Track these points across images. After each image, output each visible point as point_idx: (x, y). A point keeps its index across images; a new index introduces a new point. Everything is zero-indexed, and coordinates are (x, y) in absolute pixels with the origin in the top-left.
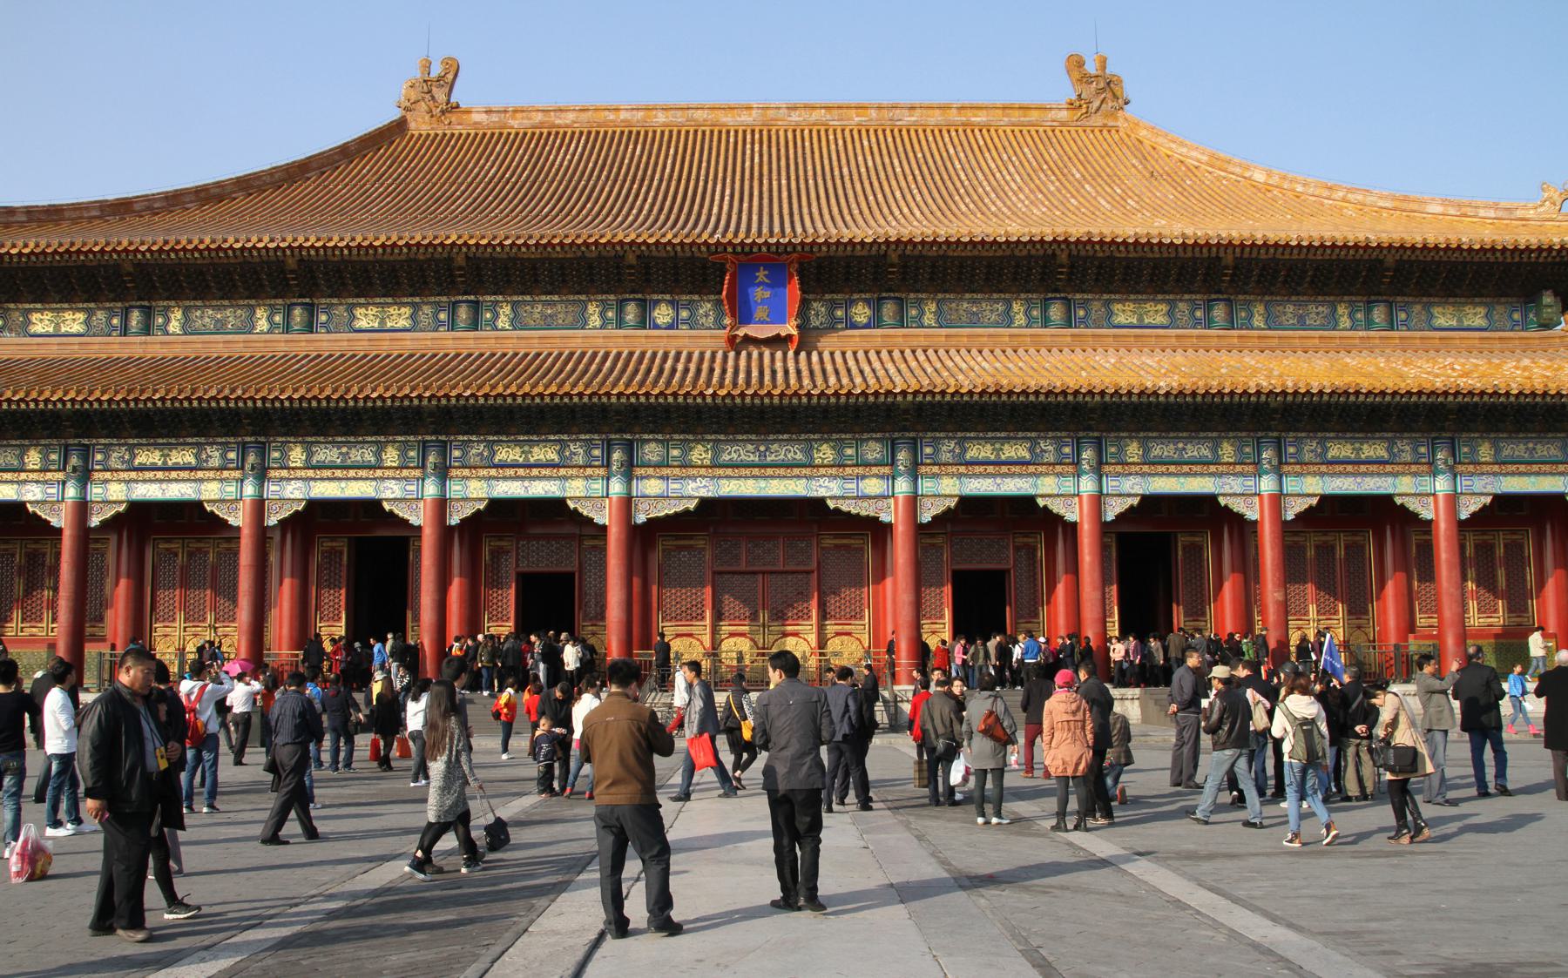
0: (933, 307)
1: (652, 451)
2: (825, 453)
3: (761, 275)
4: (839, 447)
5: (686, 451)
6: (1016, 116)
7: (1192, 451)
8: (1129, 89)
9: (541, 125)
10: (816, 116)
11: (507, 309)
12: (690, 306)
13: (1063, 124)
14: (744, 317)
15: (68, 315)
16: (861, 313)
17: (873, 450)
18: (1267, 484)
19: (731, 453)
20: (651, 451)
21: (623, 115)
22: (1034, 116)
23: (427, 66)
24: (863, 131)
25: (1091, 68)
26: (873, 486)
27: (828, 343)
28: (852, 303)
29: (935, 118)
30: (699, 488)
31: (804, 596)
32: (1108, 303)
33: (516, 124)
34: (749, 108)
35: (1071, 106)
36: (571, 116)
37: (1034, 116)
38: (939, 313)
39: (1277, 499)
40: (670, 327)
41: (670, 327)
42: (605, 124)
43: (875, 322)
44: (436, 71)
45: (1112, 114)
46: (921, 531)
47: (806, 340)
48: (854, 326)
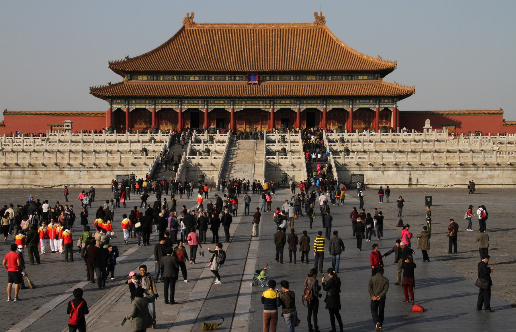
1: (237, 102)
2: (261, 102)
7: (313, 102)
8: (326, 20)
9: (211, 27)
10: (264, 26)
11: (213, 77)
12: (242, 77)
14: (250, 80)
16: (268, 78)
17: (268, 102)
18: (324, 107)
19: (248, 102)
20: (237, 102)
21: (227, 26)
22: (307, 26)
24: (274, 30)
25: (319, 15)
26: (268, 107)
27: (262, 84)
28: (266, 77)
29: (287, 26)
30: (244, 107)
31: (259, 122)
33: (206, 27)
34: (251, 24)
35: (315, 23)
36: (217, 26)
37: (307, 26)
38: (280, 78)
39: (326, 109)
41: (239, 80)
42: (223, 27)
43: (270, 80)
44: (190, 15)
45: (322, 25)
46: (274, 113)
47: (259, 84)
48: (267, 80)
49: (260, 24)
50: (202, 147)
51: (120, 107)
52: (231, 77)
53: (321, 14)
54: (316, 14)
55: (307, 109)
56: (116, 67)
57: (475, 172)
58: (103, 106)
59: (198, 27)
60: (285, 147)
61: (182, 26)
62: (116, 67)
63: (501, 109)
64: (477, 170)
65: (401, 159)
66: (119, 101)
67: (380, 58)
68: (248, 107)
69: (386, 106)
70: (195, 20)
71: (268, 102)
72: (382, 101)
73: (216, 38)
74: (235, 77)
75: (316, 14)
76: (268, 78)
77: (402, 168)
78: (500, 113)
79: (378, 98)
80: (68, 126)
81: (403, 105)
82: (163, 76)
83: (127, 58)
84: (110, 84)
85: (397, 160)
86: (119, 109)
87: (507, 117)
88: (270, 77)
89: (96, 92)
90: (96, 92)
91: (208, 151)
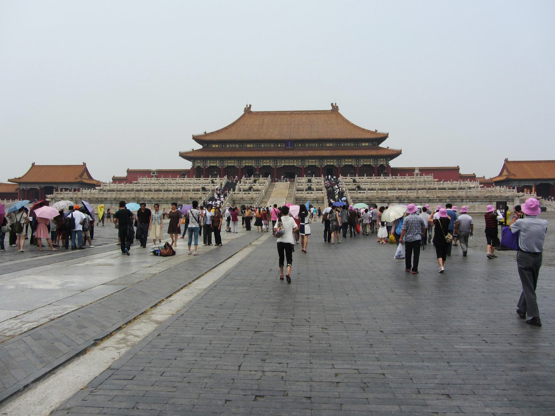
16: (300, 145)
23: (247, 105)
30: (283, 164)
49: (295, 111)
50: (247, 187)
53: (336, 104)
54: (332, 104)
55: (327, 166)
56: (197, 139)
57: (460, 203)
58: (187, 165)
61: (243, 112)
62: (197, 139)
63: (458, 166)
64: (462, 202)
65: (403, 194)
67: (376, 131)
70: (251, 110)
73: (266, 120)
74: (278, 145)
75: (332, 104)
76: (300, 145)
77: (404, 200)
78: (457, 169)
79: (376, 158)
80: (154, 173)
81: (394, 163)
83: (205, 133)
84: (193, 150)
85: (400, 194)
86: (199, 167)
87: (462, 172)
89: (184, 156)
90: (184, 156)
91: (250, 189)
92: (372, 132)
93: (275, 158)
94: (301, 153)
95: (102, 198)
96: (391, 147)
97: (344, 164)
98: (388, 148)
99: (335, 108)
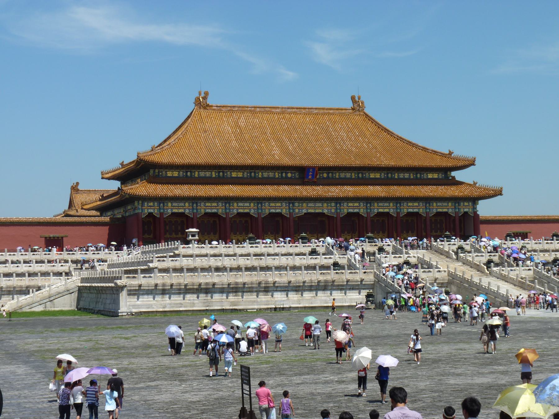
0: (338, 174)
1: (297, 204)
2: (325, 205)
3: (311, 170)
4: (327, 203)
5: (302, 205)
6: (340, 111)
8: (365, 104)
11: (260, 173)
12: (295, 173)
13: (350, 113)
15: (175, 172)
17: (333, 204)
20: (297, 204)
28: (323, 173)
30: (304, 211)
32: (369, 173)
35: (353, 109)
40: (291, 178)
44: (203, 95)
51: (152, 211)
52: (282, 173)
54: (353, 98)
59: (214, 110)
60: (492, 257)
66: (151, 204)
67: (450, 153)
68: (310, 211)
69: (466, 210)
70: (210, 101)
71: (333, 204)
72: (462, 203)
74: (286, 173)
76: (325, 175)
81: (485, 209)
82: (199, 172)
86: (150, 215)
88: (328, 174)
92: (443, 155)
93: (291, 200)
94: (335, 191)
95: (207, 284)
96: (482, 182)
97: (405, 211)
98: (475, 184)
99: (357, 105)
